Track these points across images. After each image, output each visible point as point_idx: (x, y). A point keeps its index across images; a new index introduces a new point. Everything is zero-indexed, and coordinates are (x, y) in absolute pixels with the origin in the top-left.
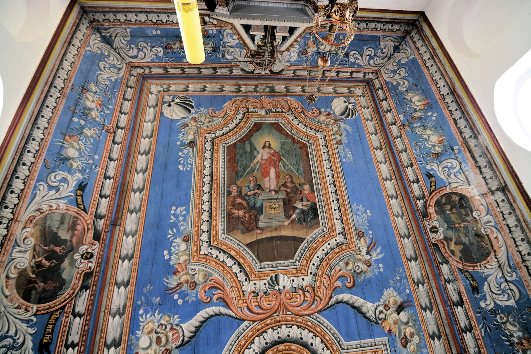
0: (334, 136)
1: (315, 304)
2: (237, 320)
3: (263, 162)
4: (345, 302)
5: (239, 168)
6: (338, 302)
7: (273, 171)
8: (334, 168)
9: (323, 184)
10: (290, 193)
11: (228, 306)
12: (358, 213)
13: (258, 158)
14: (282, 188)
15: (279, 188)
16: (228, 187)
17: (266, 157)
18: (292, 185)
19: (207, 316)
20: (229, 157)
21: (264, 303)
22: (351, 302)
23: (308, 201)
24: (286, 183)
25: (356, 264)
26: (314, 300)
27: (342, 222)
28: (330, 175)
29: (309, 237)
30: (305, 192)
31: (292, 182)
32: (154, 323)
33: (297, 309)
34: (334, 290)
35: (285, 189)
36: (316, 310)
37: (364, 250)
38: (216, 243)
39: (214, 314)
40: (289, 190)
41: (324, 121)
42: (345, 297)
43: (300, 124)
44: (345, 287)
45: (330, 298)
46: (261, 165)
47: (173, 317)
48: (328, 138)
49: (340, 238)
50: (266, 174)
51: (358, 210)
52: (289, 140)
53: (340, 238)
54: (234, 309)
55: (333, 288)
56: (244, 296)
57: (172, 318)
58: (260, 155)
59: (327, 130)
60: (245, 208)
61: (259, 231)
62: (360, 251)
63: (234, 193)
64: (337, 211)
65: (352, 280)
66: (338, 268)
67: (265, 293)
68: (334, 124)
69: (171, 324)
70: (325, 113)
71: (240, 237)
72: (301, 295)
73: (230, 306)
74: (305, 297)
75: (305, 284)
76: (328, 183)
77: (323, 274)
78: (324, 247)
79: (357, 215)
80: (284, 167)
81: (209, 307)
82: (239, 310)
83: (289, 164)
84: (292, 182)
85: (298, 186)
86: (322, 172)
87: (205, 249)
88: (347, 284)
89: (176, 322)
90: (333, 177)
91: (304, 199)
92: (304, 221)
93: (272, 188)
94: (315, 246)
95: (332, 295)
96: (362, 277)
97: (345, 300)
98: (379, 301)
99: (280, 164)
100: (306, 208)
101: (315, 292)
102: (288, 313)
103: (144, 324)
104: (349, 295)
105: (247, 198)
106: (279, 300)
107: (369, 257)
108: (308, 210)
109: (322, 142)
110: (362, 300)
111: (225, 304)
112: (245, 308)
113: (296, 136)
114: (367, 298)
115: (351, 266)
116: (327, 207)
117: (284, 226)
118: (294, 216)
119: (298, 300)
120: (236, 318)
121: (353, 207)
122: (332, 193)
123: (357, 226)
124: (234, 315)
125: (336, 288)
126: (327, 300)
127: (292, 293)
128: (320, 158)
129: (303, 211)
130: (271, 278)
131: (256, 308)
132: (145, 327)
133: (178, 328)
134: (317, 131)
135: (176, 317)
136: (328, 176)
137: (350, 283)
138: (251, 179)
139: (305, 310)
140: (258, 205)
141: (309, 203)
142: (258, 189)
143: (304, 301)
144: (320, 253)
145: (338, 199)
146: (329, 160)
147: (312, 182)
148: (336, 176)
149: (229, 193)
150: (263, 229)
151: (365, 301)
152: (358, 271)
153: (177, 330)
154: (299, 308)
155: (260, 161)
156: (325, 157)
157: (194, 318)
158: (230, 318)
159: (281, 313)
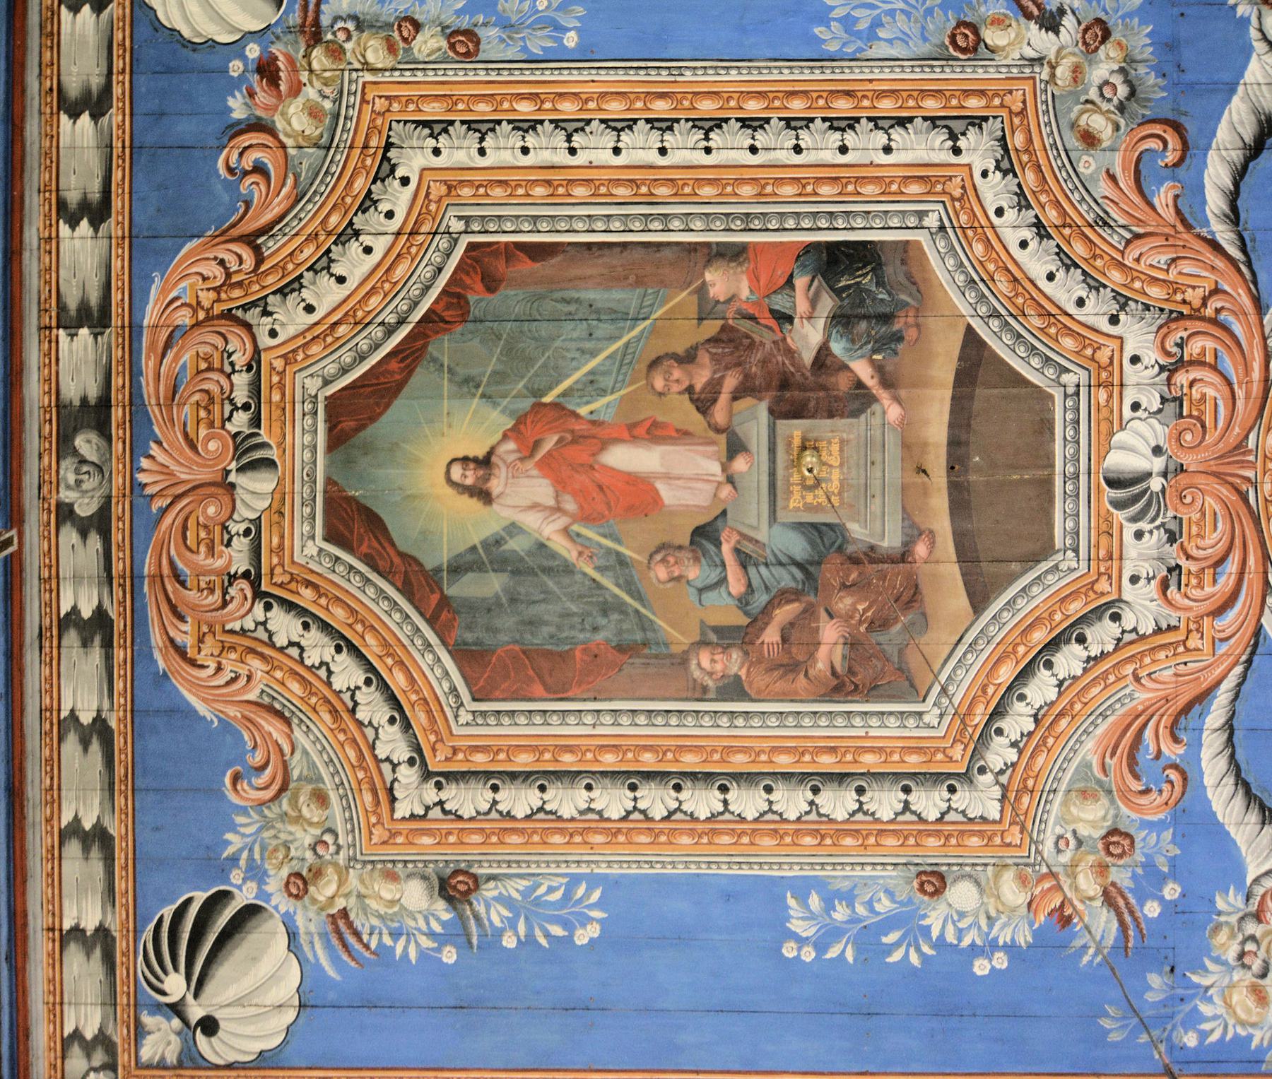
0: (416, 65)
1: (1231, 319)
2: (1256, 659)
3: (570, 505)
4: (1236, 184)
5: (600, 637)
6: (1234, 216)
7: (624, 458)
8: (615, 109)
9: (707, 192)
10: (747, 376)
11: (1204, 696)
12: (863, 26)
13: (550, 530)
14: (719, 413)
15: (718, 431)
16: (701, 693)
17: (541, 489)
18: (704, 357)
19: (1230, 780)
20: (538, 689)
21: (1208, 542)
22: (1237, 156)
23: (789, 283)
24: (690, 390)
25: (1093, 94)
26: (1214, 322)
27: (902, 122)
28: (654, 139)
29: (964, 309)
30: (745, 293)
31: (688, 358)
32: (1232, 986)
33: (1240, 404)
34: (1188, 227)
35: (724, 398)
36: (1253, 318)
37: (1039, 40)
38: (957, 752)
39: (1227, 752)
40: (731, 382)
41: (314, 112)
42: (1216, 174)
43: (337, 269)
44: (1181, 172)
45: (1215, 246)
46: (587, 518)
47: (1219, 913)
48: (433, 111)
49: (978, 150)
50: (639, 496)
51: (848, 22)
52: (443, 347)
53: (978, 150)
54: (1218, 672)
55: (1180, 228)
56: (1176, 628)
57: (1222, 919)
58: (531, 521)
59: (380, 105)
60: (809, 612)
61: (921, 550)
62: (1040, 60)
63: (733, 663)
64: (850, 139)
65: (1157, 129)
66: (1103, 188)
67: (1172, 538)
68: (336, 52)
69: (1242, 918)
70: (262, 97)
71: (937, 640)
72: (1191, 376)
73: (1204, 686)
74: (1199, 363)
75: (1151, 356)
76: (700, 158)
77: (1121, 266)
78: (1012, 239)
79: (871, 36)
80: (603, 392)
81: (1202, 774)
82: (1223, 649)
83: (589, 368)
84: (688, 358)
85: (712, 327)
86: (640, 182)
87: (982, 800)
88: (1171, 157)
89: (1240, 903)
90: (666, 125)
91: (780, 302)
92: (886, 318)
93: (715, 468)
94: (1003, 286)
95: (1204, 239)
96: (1149, 79)
97: (1227, 182)
98: (1245, 21)
99: (583, 411)
100: (827, 303)
101: (1186, 310)
102: (1251, 443)
103: (1231, 1022)
104: (1212, 155)
105: (761, 599)
106: (1201, 480)
107: (1068, 22)
108: (838, 292)
109: (459, 152)
110: (1236, 100)
111: (1197, 708)
112: (1220, 623)
113: (415, 304)
114: (1226, 77)
115: (1098, 123)
116: (826, 191)
117: (906, 424)
118: (862, 370)
119: (1210, 392)
120: (1249, 662)
121: (833, 47)
122: (753, 150)
123: (925, 49)
124: (1239, 669)
125: (1178, 212)
126: (1220, 263)
127: (1181, 416)
128: (555, 182)
129: (841, 320)
130: (1119, 505)
131: (1222, 580)
132: (1243, 1016)
133: (1259, 891)
134: (386, 171)
135: (1220, 904)
136: (663, 151)
137: (1165, 143)
138: (661, 572)
139: (1248, 370)
140: (798, 547)
141: (801, 282)
142: (718, 544)
143: (1214, 368)
144: (1037, 263)
145: (788, 121)
146: (570, 128)
147: (692, 248)
148: (661, 108)
149: (734, 689)
150: (914, 532)
151: (1241, 89)
152: (1123, 91)
153: (1263, 896)
154: (1240, 393)
155: (562, 521)
156: (548, 149)
157: (1232, 830)
158: (1245, 688)
159: (1250, 474)
